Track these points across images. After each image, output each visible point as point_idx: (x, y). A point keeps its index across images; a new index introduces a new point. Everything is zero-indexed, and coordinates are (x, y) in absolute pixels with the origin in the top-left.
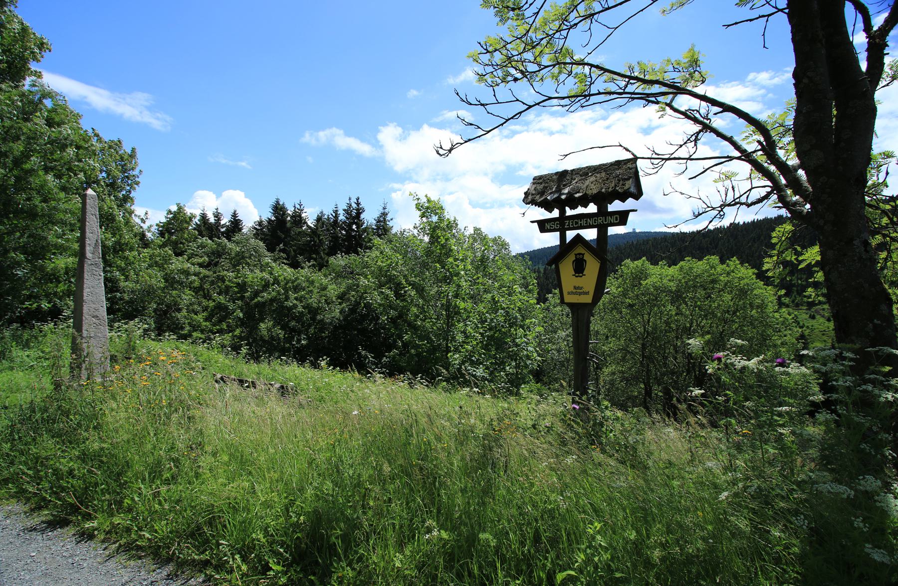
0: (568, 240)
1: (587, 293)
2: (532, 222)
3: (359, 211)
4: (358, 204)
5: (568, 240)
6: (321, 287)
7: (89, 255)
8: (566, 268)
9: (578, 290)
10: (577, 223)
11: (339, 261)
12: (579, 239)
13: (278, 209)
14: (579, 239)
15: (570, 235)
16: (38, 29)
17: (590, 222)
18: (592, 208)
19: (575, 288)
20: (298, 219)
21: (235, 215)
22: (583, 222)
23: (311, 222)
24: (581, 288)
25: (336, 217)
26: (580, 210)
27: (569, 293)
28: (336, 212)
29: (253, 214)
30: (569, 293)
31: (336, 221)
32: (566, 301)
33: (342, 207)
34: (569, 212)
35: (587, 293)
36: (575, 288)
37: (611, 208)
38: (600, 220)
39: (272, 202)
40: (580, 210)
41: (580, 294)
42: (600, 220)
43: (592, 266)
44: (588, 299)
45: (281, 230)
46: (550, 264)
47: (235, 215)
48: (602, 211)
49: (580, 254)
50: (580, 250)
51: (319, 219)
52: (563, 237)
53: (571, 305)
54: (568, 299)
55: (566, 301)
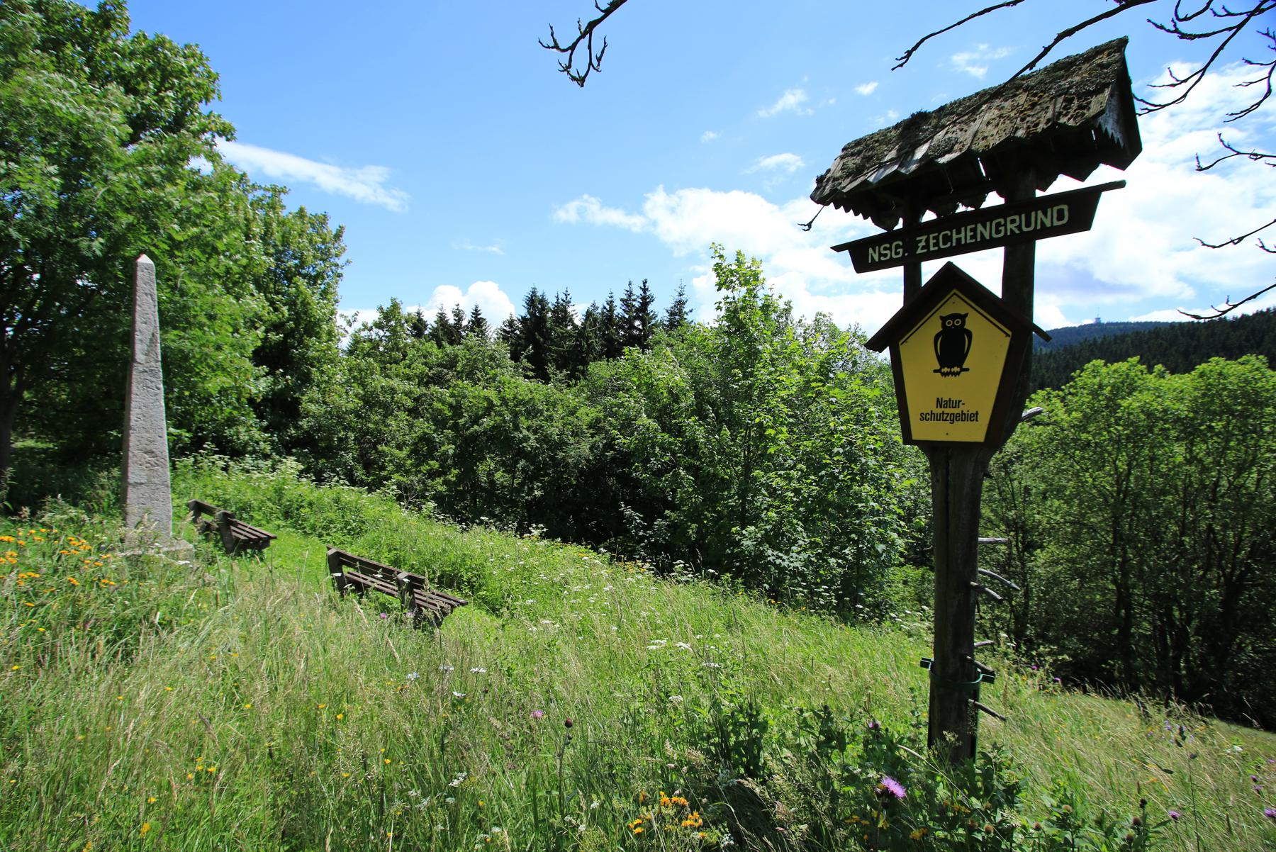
0: (925, 279)
1: (973, 417)
2: (838, 248)
3: (646, 301)
4: (645, 290)
5: (925, 279)
8: (921, 348)
9: (947, 410)
10: (947, 239)
11: (601, 369)
13: (534, 302)
14: (951, 276)
15: (930, 269)
17: (984, 231)
19: (939, 403)
20: (562, 314)
21: (476, 312)
22: (965, 235)
23: (578, 321)
24: (957, 404)
25: (611, 310)
27: (923, 417)
28: (611, 303)
29: (502, 309)
30: (923, 417)
32: (914, 437)
33: (620, 294)
35: (973, 417)
36: (939, 403)
38: (1011, 225)
39: (526, 292)
41: (954, 418)
42: (1011, 225)
43: (989, 347)
44: (975, 432)
47: (476, 312)
50: (955, 305)
51: (589, 315)
52: (912, 277)
53: (930, 448)
54: (921, 431)
55: (914, 437)
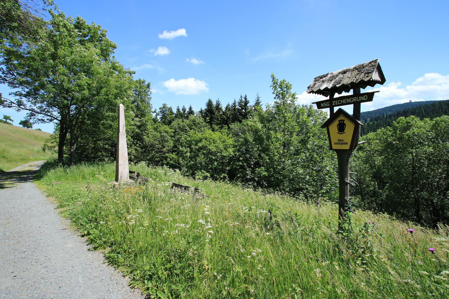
0: (335, 111)
1: (347, 143)
2: (313, 103)
3: (246, 103)
4: (246, 99)
5: (335, 111)
6: (221, 141)
7: (121, 130)
8: (334, 127)
9: (341, 142)
10: (340, 102)
11: (235, 126)
12: (340, 111)
13: (210, 104)
14: (340, 111)
15: (336, 109)
16: (113, 42)
17: (349, 101)
18: (351, 93)
19: (339, 140)
20: (218, 107)
21: (190, 108)
22: (344, 101)
23: (224, 109)
24: (343, 140)
25: (235, 106)
26: (344, 94)
27: (335, 144)
28: (234, 104)
29: (199, 106)
30: (335, 144)
31: (235, 109)
32: (333, 148)
33: (238, 100)
34: (336, 95)
35: (347, 143)
36: (339, 140)
37: (362, 91)
38: (355, 99)
39: (207, 101)
40: (344, 94)
41: (342, 144)
42: (355, 99)
43: (349, 128)
44: (347, 147)
45: (212, 114)
46: (323, 127)
47: (190, 108)
48: (357, 94)
49: (341, 120)
50: (342, 118)
51: (227, 108)
52: (332, 111)
53: (337, 151)
54: (334, 147)
55: (333, 148)
